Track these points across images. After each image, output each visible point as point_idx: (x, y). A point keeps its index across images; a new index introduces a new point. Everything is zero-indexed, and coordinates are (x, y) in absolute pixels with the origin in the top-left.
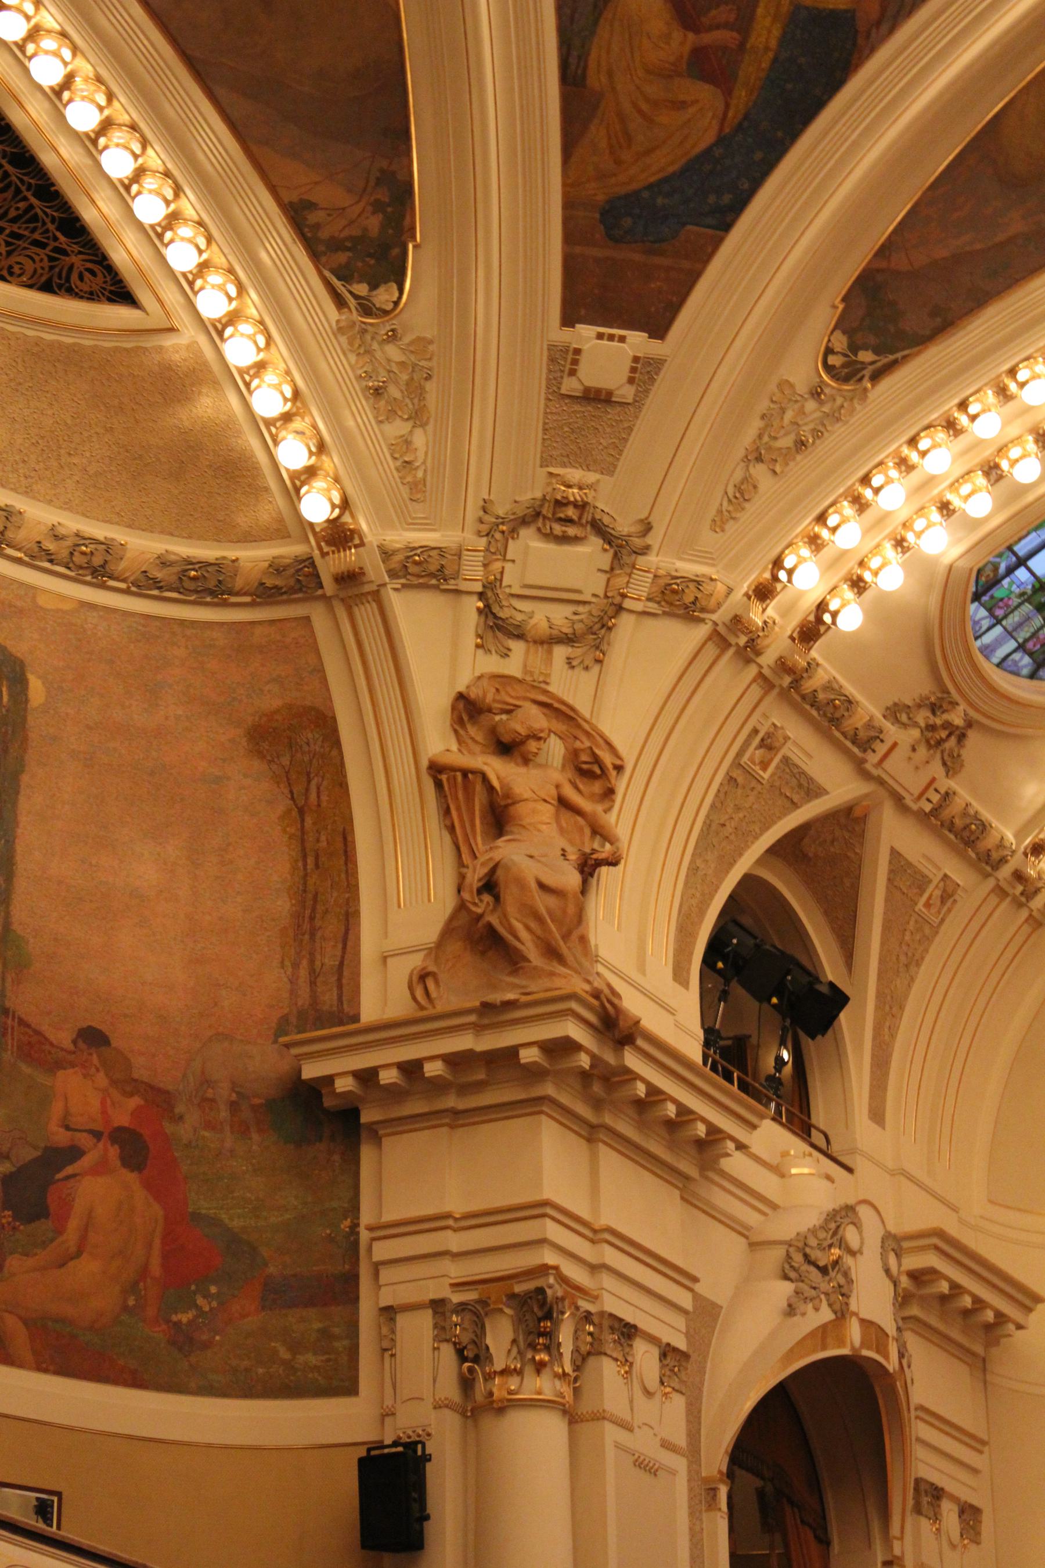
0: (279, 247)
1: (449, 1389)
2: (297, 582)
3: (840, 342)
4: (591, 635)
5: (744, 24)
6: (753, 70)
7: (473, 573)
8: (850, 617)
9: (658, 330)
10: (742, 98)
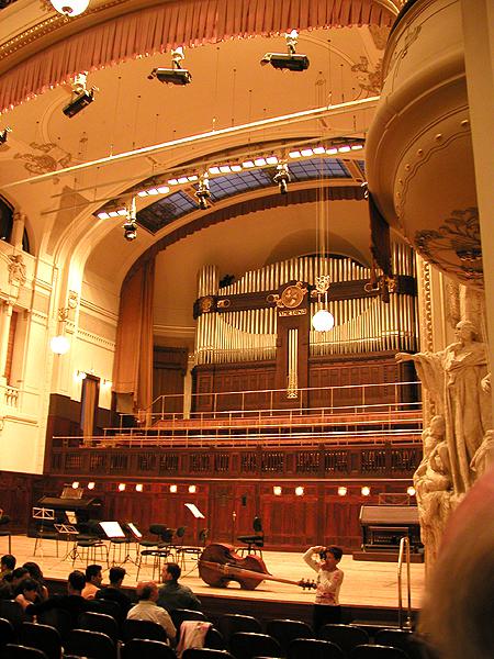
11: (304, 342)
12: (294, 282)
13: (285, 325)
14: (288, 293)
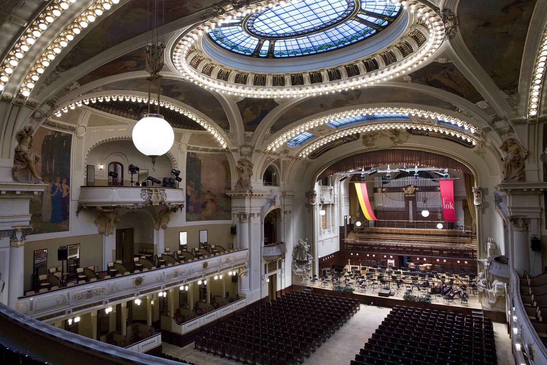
0: (218, 127)
1: (238, 221)
2: (224, 151)
4: (250, 155)
7: (239, 151)
8: (274, 150)
9: (254, 132)
10: (258, 115)
11: (415, 206)
12: (410, 186)
13: (407, 199)
14: (409, 189)
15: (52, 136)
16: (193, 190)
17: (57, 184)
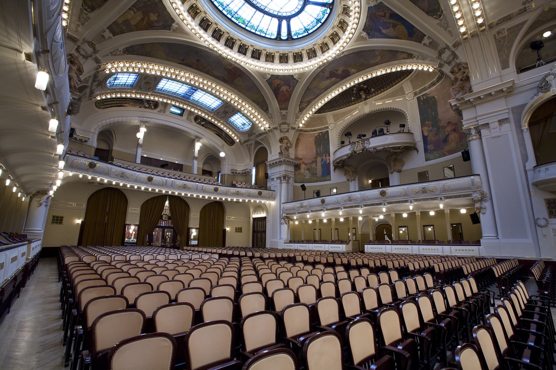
3: (435, 16)
5: (390, 23)
6: (395, 22)
15: (319, 135)
16: (431, 128)
17: (324, 158)
